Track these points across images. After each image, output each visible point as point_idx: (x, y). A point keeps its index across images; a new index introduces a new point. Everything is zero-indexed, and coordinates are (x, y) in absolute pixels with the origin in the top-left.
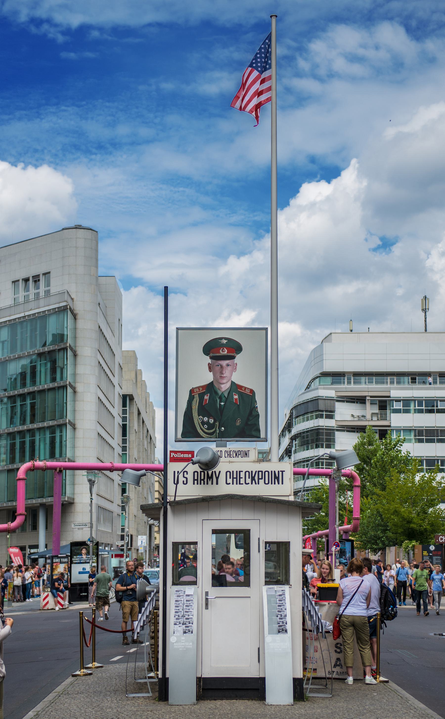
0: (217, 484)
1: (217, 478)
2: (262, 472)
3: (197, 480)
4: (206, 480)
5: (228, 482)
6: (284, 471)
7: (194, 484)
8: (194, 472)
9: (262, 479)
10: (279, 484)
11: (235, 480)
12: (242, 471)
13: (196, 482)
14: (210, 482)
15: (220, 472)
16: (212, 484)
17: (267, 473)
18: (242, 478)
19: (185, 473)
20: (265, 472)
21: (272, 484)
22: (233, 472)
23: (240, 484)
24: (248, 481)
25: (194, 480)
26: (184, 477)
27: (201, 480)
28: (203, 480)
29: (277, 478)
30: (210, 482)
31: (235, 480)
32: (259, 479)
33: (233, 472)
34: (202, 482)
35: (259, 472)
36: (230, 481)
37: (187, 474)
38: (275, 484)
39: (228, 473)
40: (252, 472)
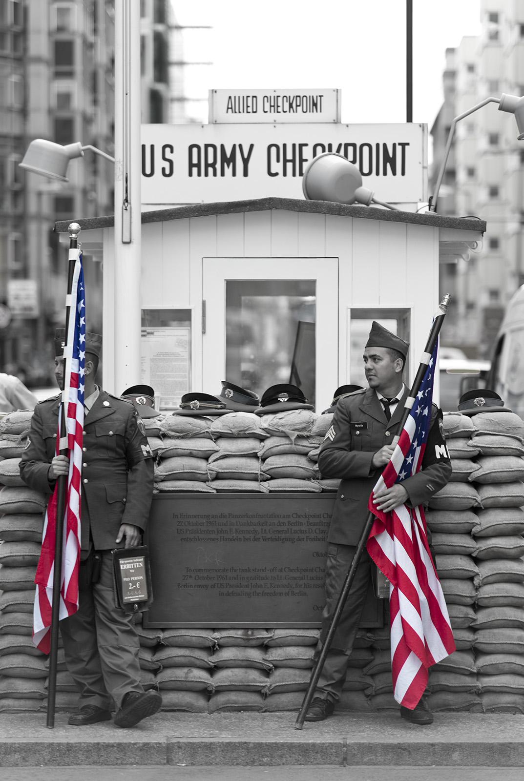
0: (246, 174)
1: (246, 162)
2: (354, 145)
3: (198, 166)
4: (218, 166)
5: (273, 171)
6: (408, 144)
7: (190, 174)
8: (191, 148)
10: (394, 173)
11: (289, 165)
12: (306, 145)
13: (195, 170)
14: (228, 171)
15: (252, 146)
16: (234, 174)
17: (366, 149)
18: (306, 160)
19: (168, 150)
20: (362, 146)
21: (378, 174)
22: (285, 145)
23: (301, 174)
25: (191, 165)
26: (164, 158)
27: (207, 165)
28: (213, 165)
29: (390, 160)
30: (228, 171)
31: (289, 165)
33: (285, 145)
34: (210, 170)
35: (347, 145)
36: (277, 167)
37: (172, 152)
38: (385, 174)
39: (274, 150)
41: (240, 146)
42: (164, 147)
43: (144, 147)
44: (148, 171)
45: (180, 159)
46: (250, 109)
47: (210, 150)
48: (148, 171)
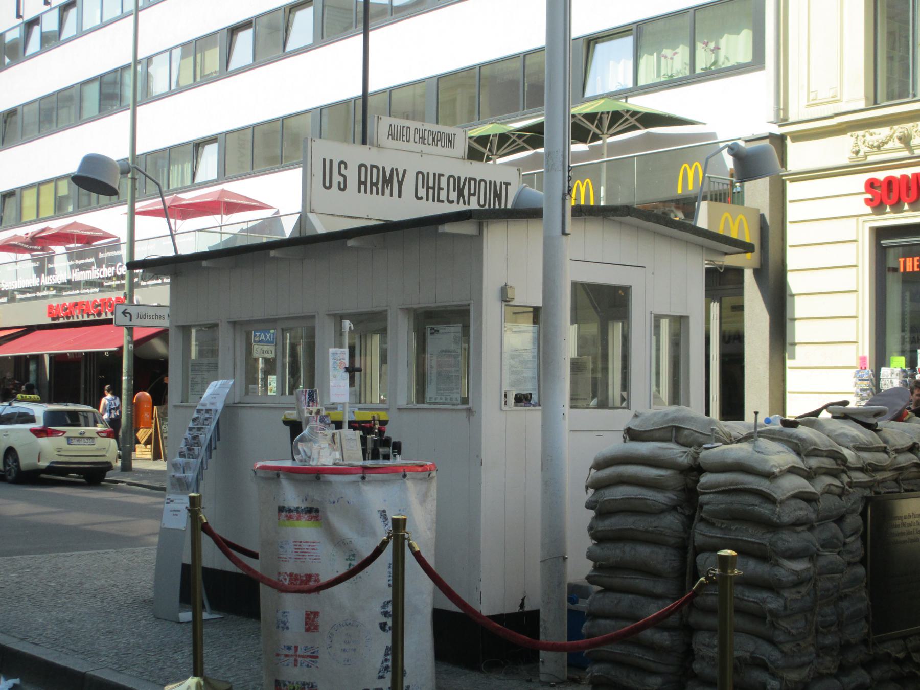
0: (400, 196)
1: (400, 184)
2: (475, 180)
3: (365, 183)
4: (380, 186)
5: (419, 195)
7: (359, 191)
8: (361, 166)
9: (474, 195)
11: (431, 191)
12: (443, 175)
13: (363, 187)
14: (387, 191)
15: (405, 171)
16: (391, 195)
17: (483, 184)
18: (442, 189)
19: (343, 166)
20: (481, 181)
22: (428, 174)
23: (439, 201)
24: (453, 196)
25: (360, 183)
26: (340, 174)
27: (372, 184)
28: (376, 184)
30: (387, 191)
31: (431, 191)
32: (470, 194)
34: (374, 188)
35: (470, 179)
36: (422, 192)
37: (346, 168)
39: (420, 176)
40: (459, 178)
41: (397, 170)
42: (341, 163)
43: (324, 160)
44: (327, 184)
45: (352, 175)
46: (405, 138)
47: (375, 170)
48: (327, 184)
